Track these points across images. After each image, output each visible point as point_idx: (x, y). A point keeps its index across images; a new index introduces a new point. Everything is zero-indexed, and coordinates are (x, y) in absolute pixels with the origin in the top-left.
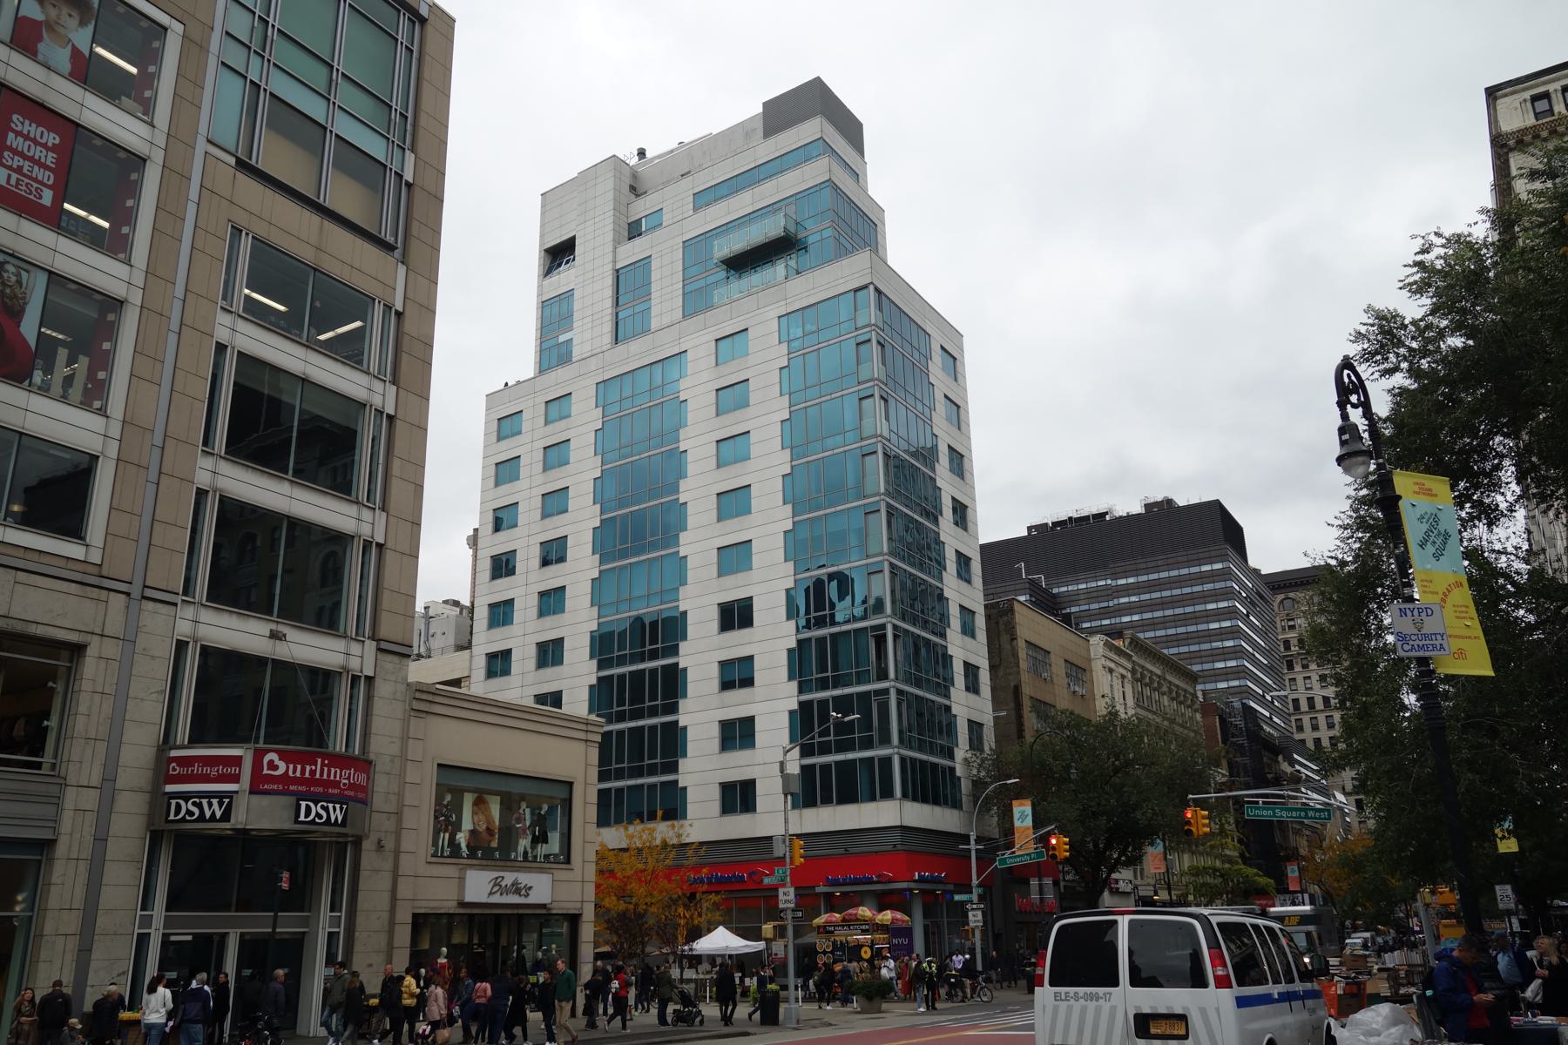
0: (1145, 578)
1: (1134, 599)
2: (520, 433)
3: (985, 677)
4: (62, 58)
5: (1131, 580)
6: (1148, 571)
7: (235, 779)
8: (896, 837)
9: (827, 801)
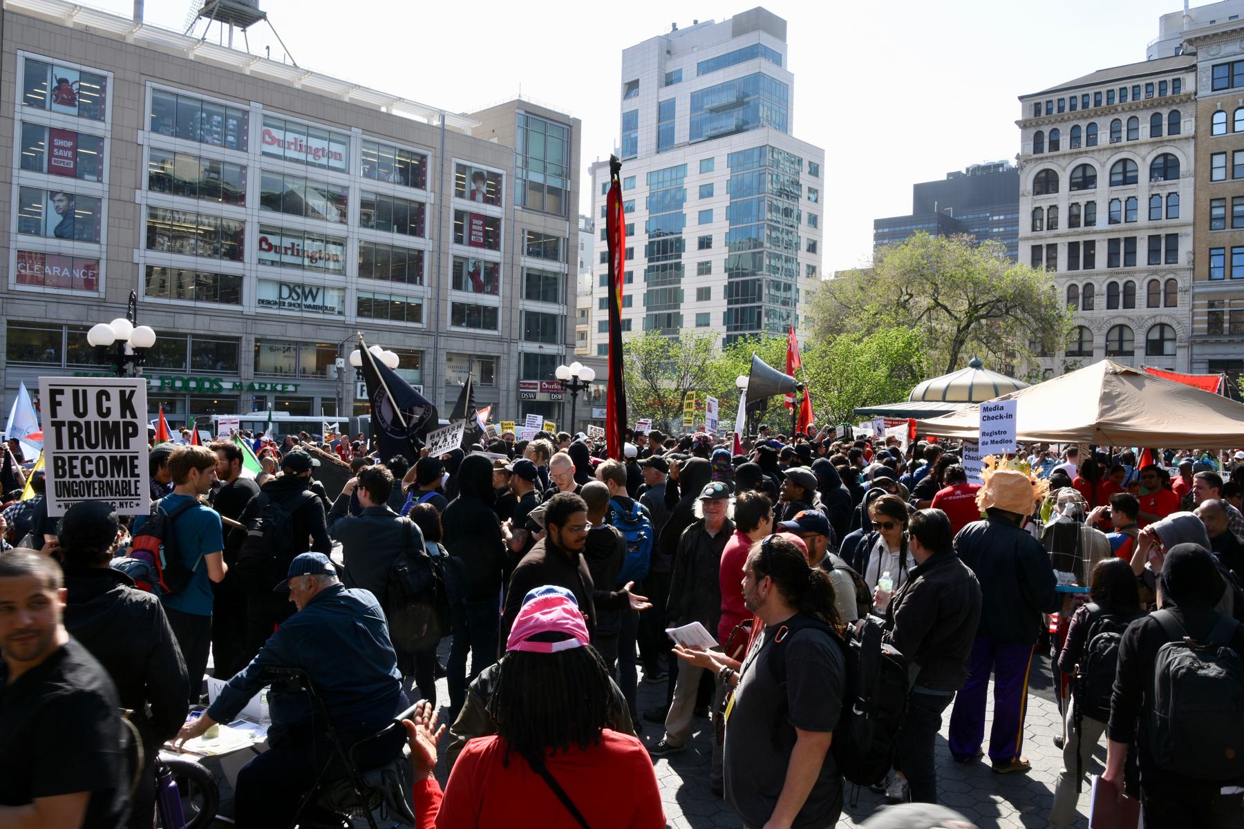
4: (474, 187)
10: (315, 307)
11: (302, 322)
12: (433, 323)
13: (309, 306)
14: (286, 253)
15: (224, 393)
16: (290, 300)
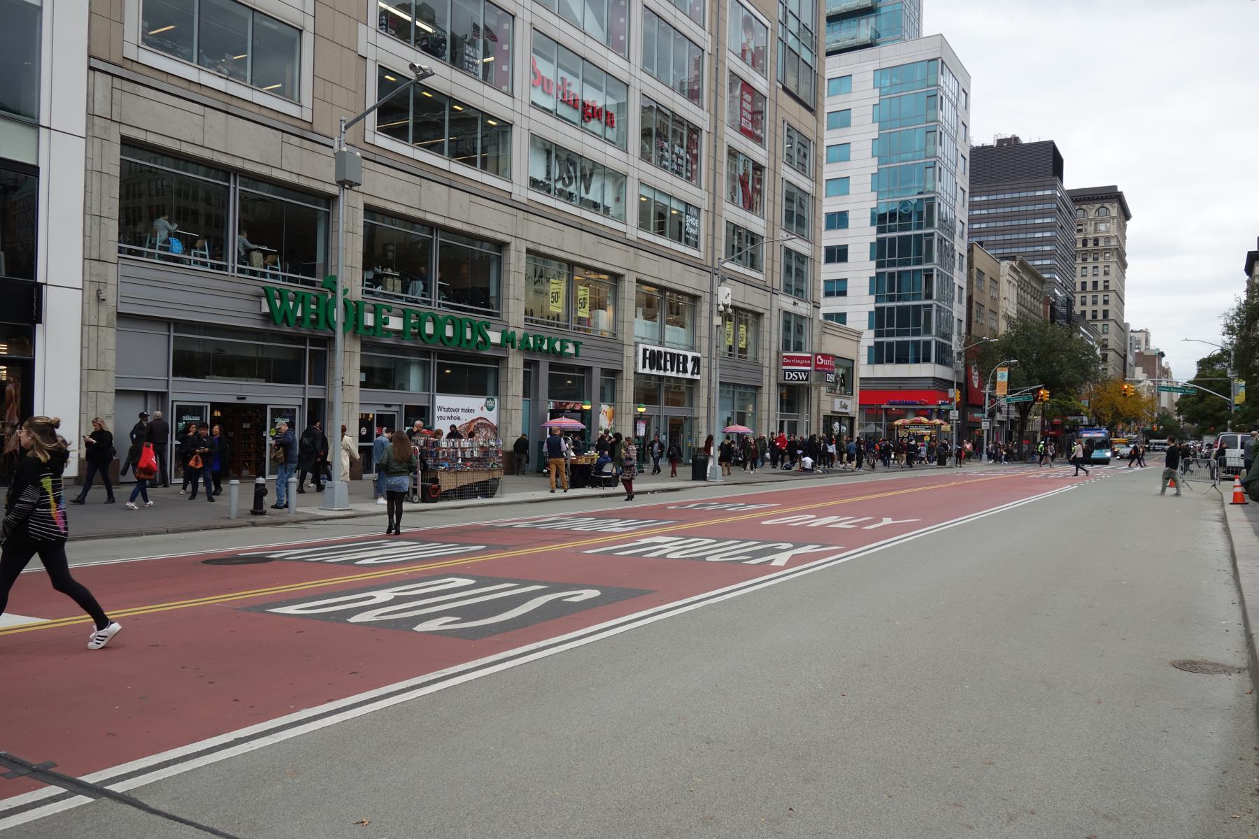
0: (993, 197)
1: (984, 212)
5: (984, 198)
6: (997, 192)
8: (931, 382)
9: (890, 361)
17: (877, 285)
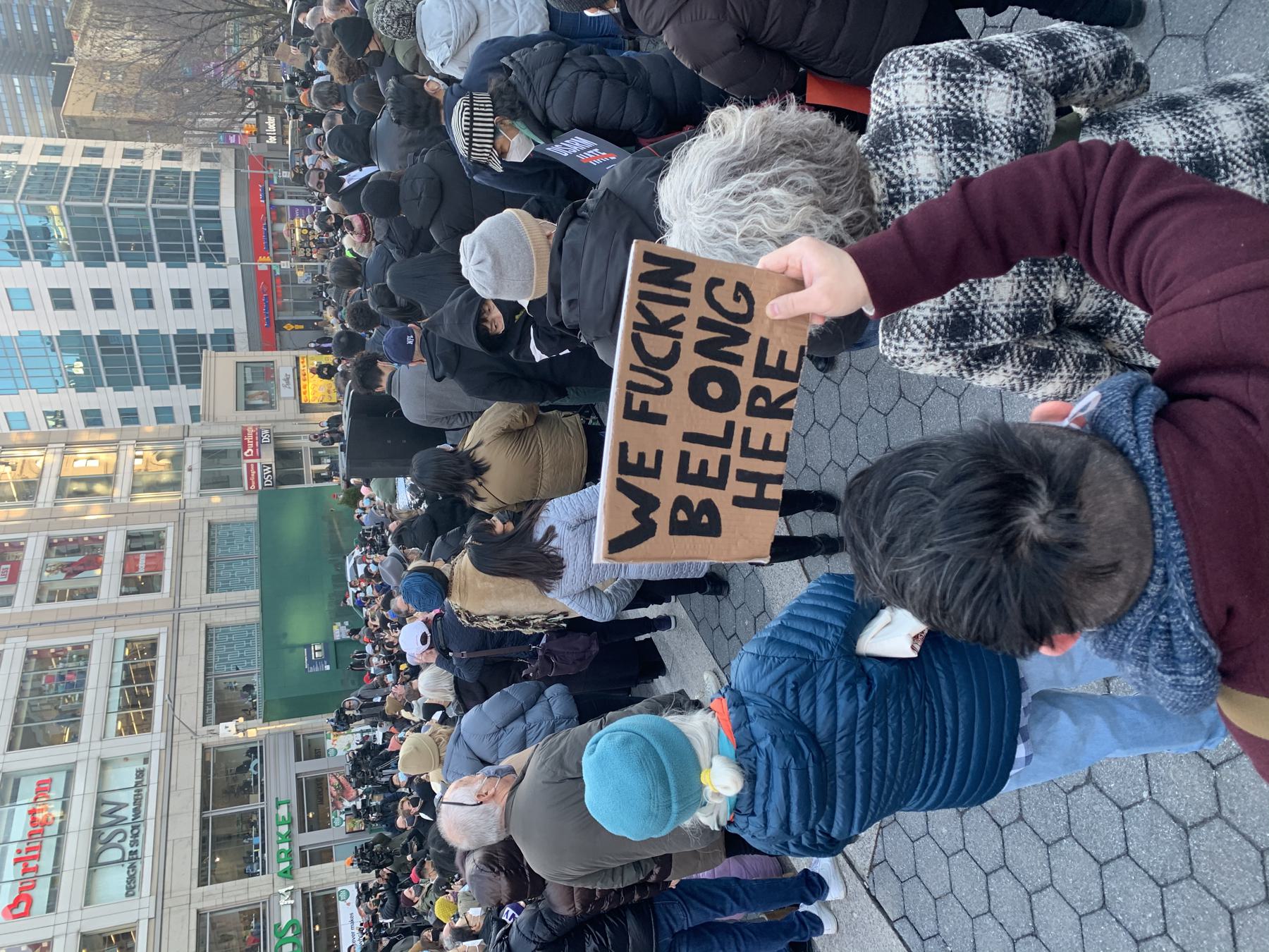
2: (24, 413)
3: (131, 145)
7: (255, 464)
10: (137, 801)
11: (165, 816)
12: (157, 618)
13: (137, 812)
14: (36, 869)
15: (299, 917)
16: (126, 844)
17: (136, 259)
